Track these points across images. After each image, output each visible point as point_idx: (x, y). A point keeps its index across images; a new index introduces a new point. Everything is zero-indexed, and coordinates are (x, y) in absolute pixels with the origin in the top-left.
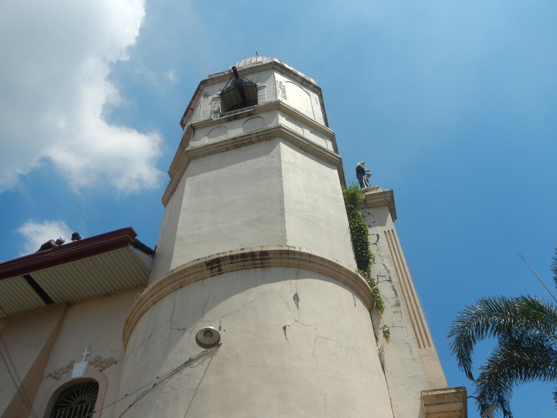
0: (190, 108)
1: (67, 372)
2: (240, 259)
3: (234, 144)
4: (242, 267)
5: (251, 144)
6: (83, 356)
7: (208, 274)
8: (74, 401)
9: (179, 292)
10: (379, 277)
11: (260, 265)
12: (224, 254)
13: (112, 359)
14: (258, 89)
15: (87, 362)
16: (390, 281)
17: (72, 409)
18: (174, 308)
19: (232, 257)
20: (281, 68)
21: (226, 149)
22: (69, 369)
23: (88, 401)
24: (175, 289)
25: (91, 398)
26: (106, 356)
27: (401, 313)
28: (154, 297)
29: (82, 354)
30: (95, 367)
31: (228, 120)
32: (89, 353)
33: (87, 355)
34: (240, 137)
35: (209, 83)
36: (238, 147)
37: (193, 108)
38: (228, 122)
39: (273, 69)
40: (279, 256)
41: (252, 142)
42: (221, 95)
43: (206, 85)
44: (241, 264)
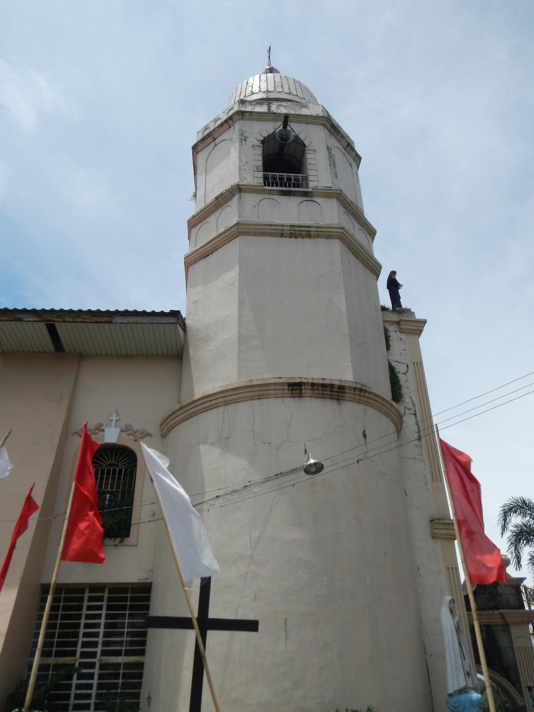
0: (212, 136)
1: (96, 434)
2: (320, 388)
3: (290, 232)
4: (321, 396)
5: (307, 238)
6: (112, 420)
7: (289, 394)
8: (105, 464)
9: (257, 403)
10: (406, 409)
11: (336, 397)
12: (307, 380)
13: (146, 431)
14: (307, 152)
15: (119, 430)
16: (415, 414)
17: (103, 471)
18: (254, 418)
19: (313, 385)
20: (331, 126)
21: (281, 234)
22: (97, 431)
23: (121, 466)
24: (252, 398)
25: (121, 464)
26: (137, 426)
27: (422, 448)
28: (228, 398)
29: (111, 419)
30: (129, 435)
31: (281, 194)
32: (118, 418)
33: (116, 420)
34: (298, 226)
35: (246, 116)
36: (294, 236)
37: (215, 138)
38: (280, 195)
39: (323, 125)
40: (352, 392)
41: (310, 236)
42: (263, 142)
43: (242, 118)
44: (321, 392)
